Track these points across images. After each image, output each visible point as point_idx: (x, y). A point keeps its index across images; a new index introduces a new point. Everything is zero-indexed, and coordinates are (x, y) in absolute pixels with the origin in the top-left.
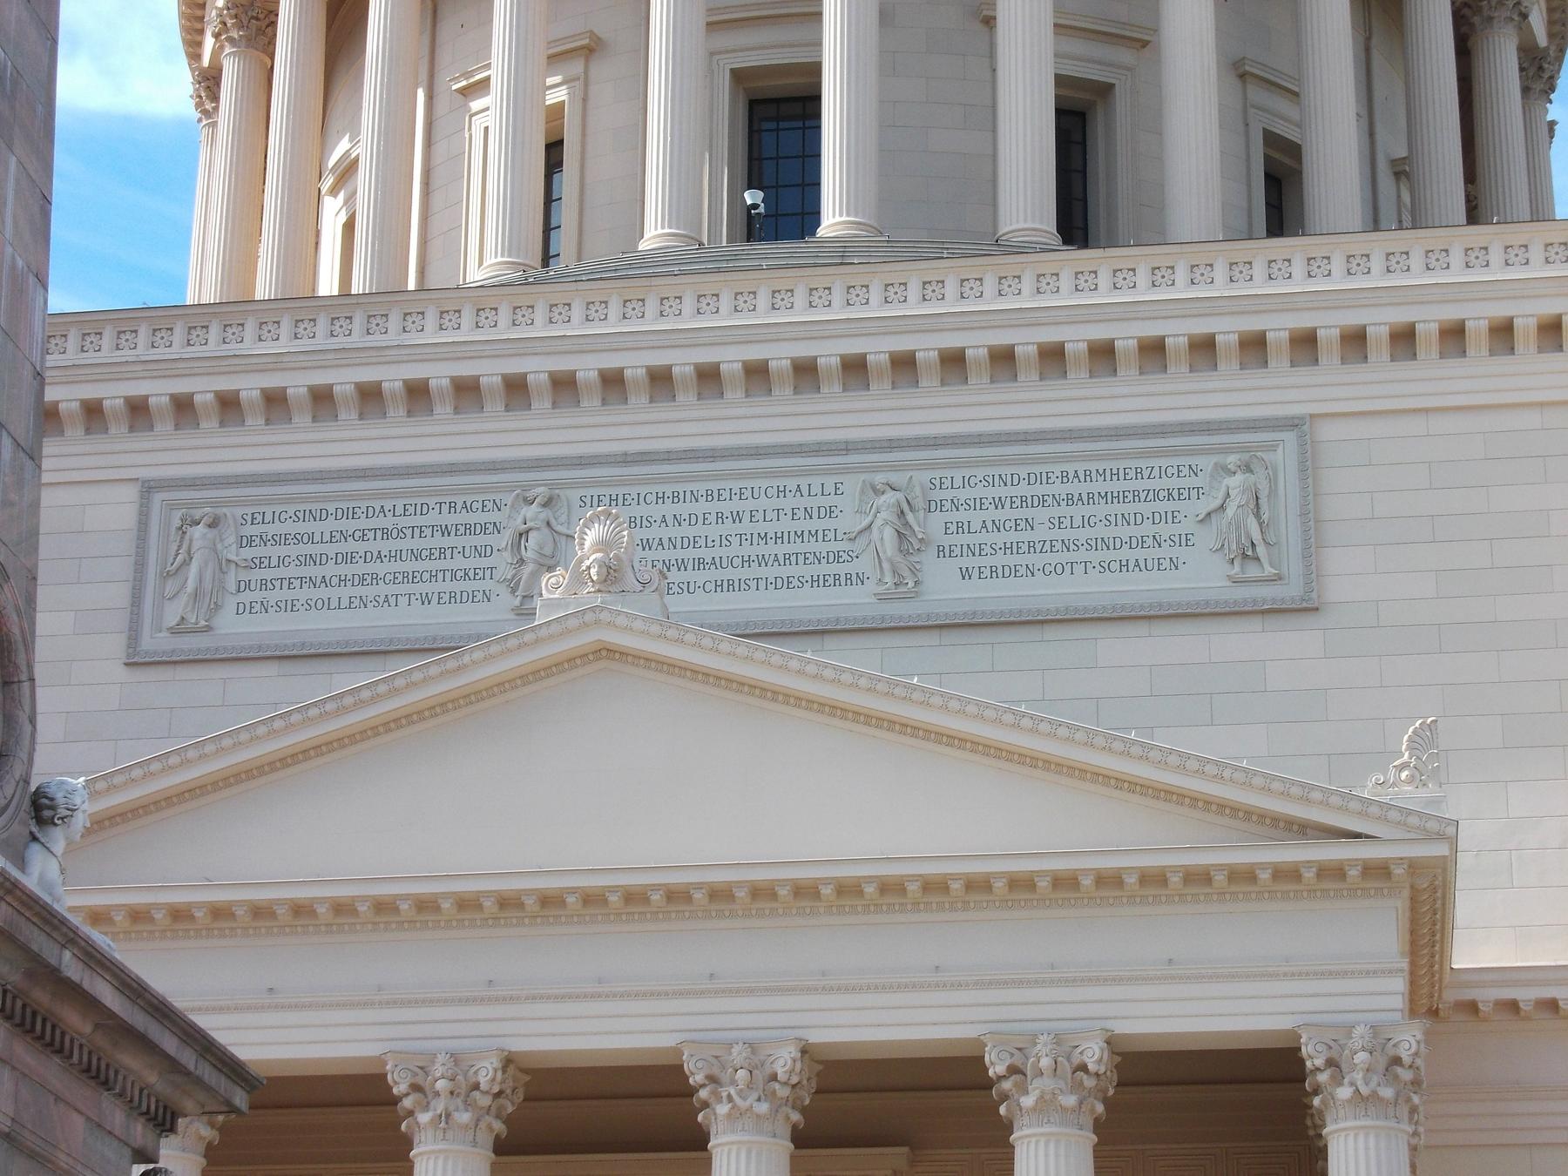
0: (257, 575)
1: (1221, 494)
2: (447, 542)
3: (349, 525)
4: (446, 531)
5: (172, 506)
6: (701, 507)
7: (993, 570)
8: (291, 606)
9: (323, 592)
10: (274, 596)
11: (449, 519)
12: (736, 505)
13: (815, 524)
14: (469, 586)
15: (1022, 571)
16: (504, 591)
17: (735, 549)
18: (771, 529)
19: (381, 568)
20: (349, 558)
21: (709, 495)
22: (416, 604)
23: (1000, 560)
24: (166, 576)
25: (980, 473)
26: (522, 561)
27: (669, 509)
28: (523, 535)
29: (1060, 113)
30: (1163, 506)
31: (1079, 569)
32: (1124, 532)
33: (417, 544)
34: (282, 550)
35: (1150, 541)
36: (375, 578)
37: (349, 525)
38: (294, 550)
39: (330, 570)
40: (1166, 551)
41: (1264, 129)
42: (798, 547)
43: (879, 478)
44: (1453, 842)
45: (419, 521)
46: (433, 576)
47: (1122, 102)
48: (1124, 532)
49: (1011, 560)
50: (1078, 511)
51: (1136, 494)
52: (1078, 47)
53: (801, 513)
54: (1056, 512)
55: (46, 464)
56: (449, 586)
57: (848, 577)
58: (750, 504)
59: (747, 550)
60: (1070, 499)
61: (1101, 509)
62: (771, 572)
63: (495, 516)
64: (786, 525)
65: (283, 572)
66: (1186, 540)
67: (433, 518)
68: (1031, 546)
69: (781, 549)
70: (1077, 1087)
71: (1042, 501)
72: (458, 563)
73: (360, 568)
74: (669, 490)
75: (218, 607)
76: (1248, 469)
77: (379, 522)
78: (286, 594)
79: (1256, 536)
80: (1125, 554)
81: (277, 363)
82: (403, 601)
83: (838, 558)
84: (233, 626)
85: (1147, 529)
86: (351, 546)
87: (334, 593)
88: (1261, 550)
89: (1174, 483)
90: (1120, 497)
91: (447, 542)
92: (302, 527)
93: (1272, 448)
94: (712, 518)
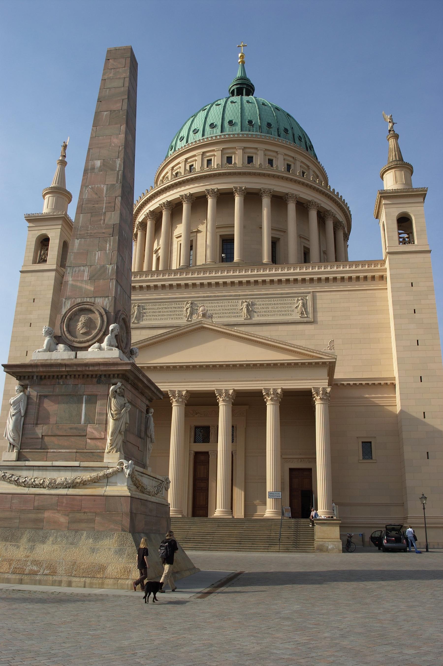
1: (298, 303)
2: (175, 310)
4: (175, 308)
6: (216, 304)
7: (262, 315)
8: (151, 319)
9: (156, 317)
12: (221, 304)
13: (234, 307)
14: (179, 317)
15: (267, 315)
17: (221, 311)
18: (227, 308)
19: (165, 314)
20: (160, 312)
21: (217, 303)
22: (171, 319)
23: (263, 313)
25: (260, 300)
27: (211, 305)
28: (187, 309)
29: (272, 242)
30: (289, 305)
31: (276, 315)
32: (283, 309)
33: (171, 310)
34: (150, 311)
35: (287, 311)
36: (164, 315)
38: (151, 311)
39: (157, 314)
40: (290, 313)
41: (304, 246)
42: (231, 311)
43: (244, 301)
44: (336, 359)
46: (173, 315)
47: (282, 242)
48: (283, 309)
49: (265, 314)
50: (276, 306)
51: (285, 303)
52: (274, 232)
53: (232, 306)
54: (272, 306)
55: (132, 296)
56: (176, 317)
57: (239, 316)
58: (224, 304)
59: (223, 311)
60: (274, 304)
61: (279, 306)
62: (227, 315)
63: (183, 306)
64: (229, 307)
66: (293, 311)
67: (173, 306)
68: (268, 311)
69: (229, 311)
70: (277, 396)
71: (270, 304)
72: (177, 313)
73: (162, 314)
74: (211, 302)
76: (302, 299)
77: (165, 306)
79: (304, 311)
80: (283, 313)
83: (238, 313)
85: (287, 309)
86: (160, 310)
87: (157, 317)
88: (304, 313)
89: (291, 302)
90: (282, 304)
91: (175, 310)
93: (307, 296)
94: (218, 306)
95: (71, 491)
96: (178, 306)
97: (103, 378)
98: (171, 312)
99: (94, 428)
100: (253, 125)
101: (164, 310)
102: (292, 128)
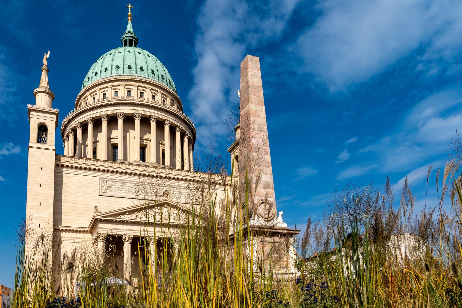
0: (111, 188)
2: (129, 188)
3: (119, 185)
4: (128, 187)
5: (102, 180)
9: (117, 191)
10: (113, 191)
11: (129, 186)
19: (123, 189)
20: (120, 188)
24: (103, 187)
33: (126, 188)
37: (119, 185)
39: (118, 189)
65: (113, 188)
67: (127, 185)
72: (130, 190)
75: (107, 191)
77: (122, 185)
78: (114, 191)
81: (113, 167)
84: (109, 193)
86: (119, 187)
87: (118, 191)
91: (129, 188)
92: (115, 184)
98: (126, 189)
100: (154, 74)
101: (122, 187)
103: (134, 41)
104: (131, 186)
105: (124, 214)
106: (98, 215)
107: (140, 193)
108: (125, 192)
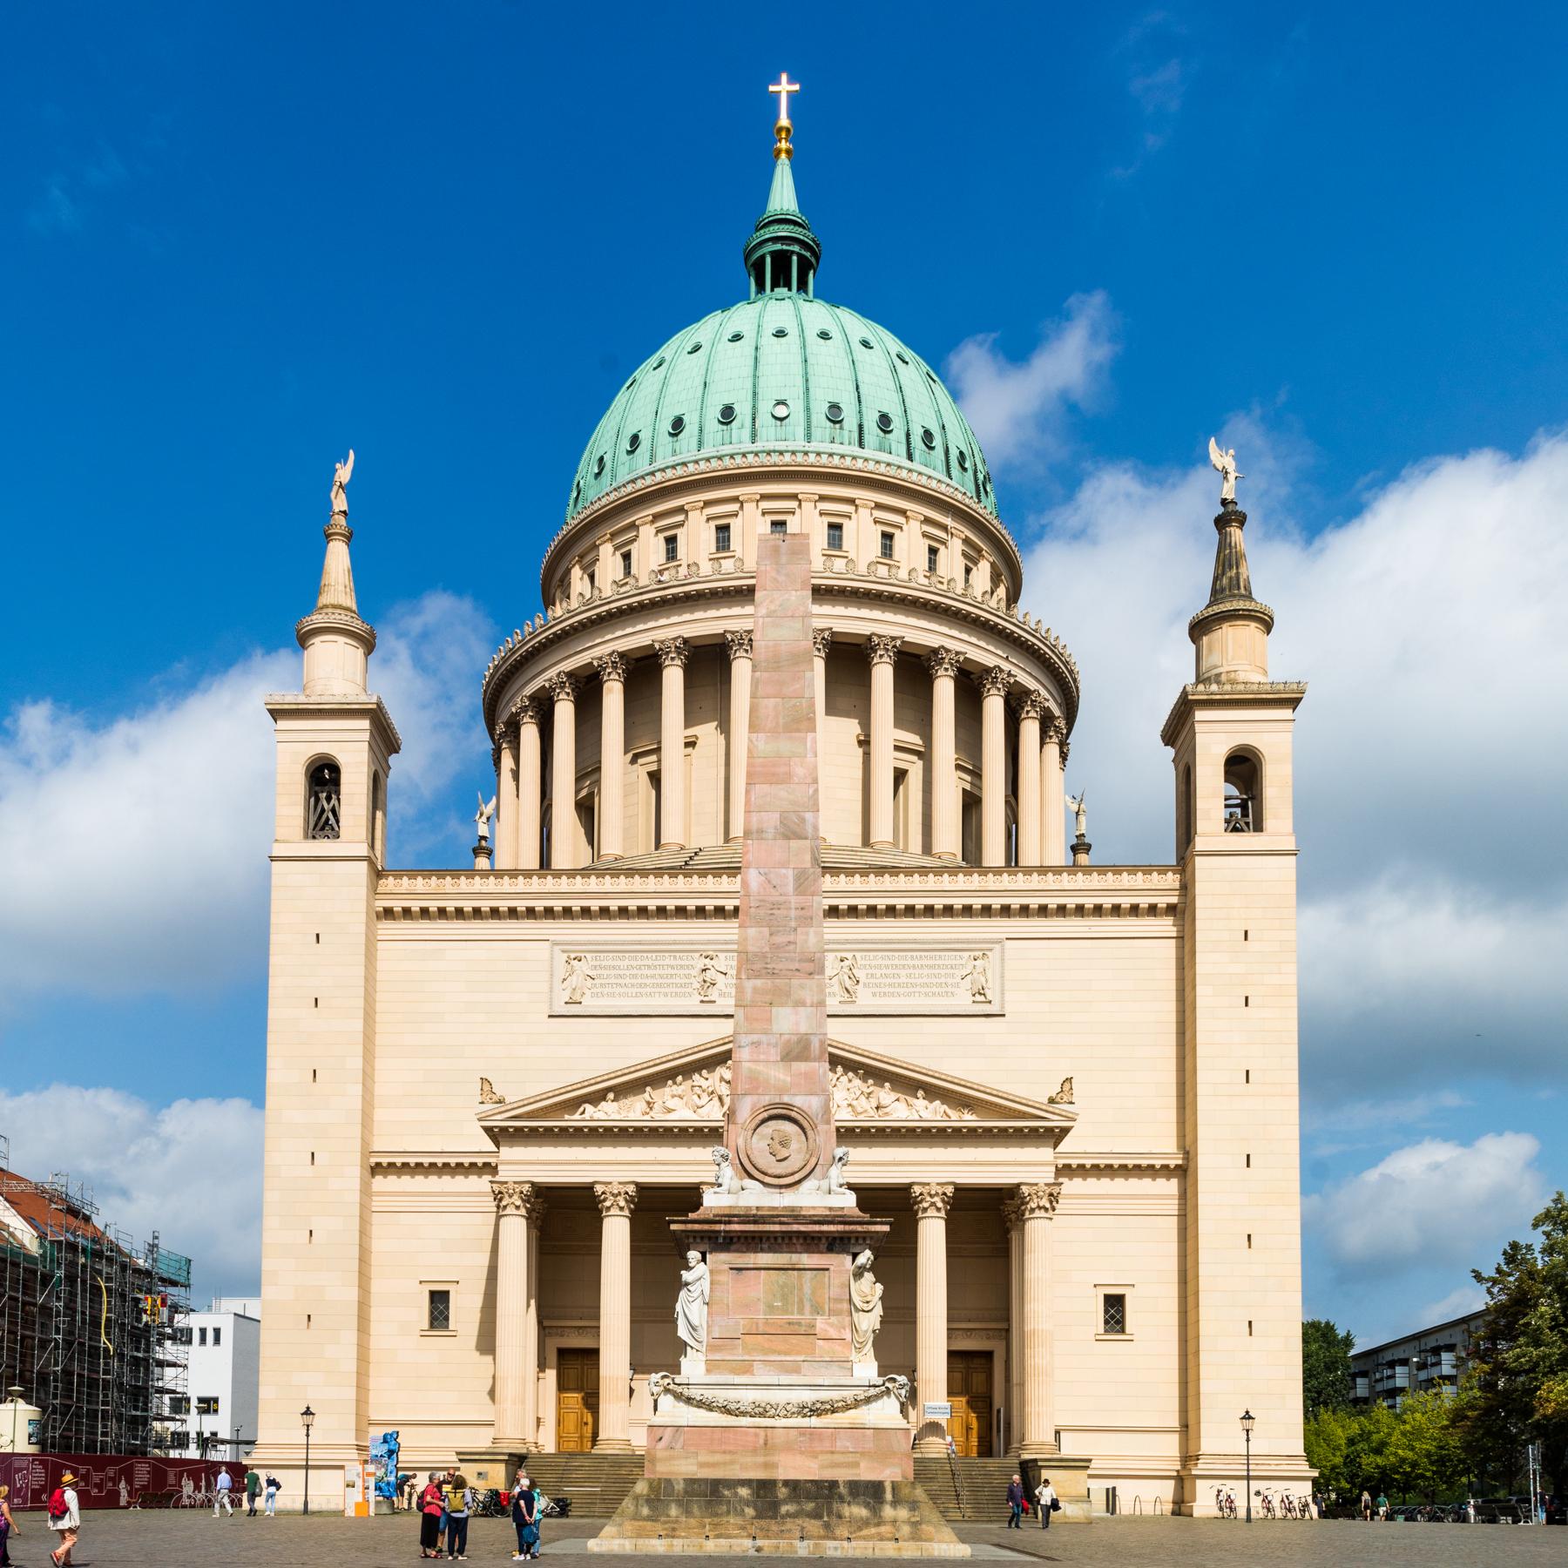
3: (632, 963)
4: (672, 967)
11: (673, 962)
14: (683, 990)
16: (695, 992)
22: (662, 996)
26: (705, 981)
45: (661, 963)
56: (674, 990)
67: (667, 962)
72: (678, 980)
73: (640, 981)
77: (643, 963)
82: (657, 995)
91: (673, 972)
95: (814, 1421)
96: (679, 962)
97: (838, 1241)
98: (661, 976)
99: (828, 1324)
100: (841, 422)
102: (943, 426)
103: (795, 258)
104: (683, 963)
105: (596, 1098)
106: (491, 1113)
107: (723, 988)
108: (659, 990)
